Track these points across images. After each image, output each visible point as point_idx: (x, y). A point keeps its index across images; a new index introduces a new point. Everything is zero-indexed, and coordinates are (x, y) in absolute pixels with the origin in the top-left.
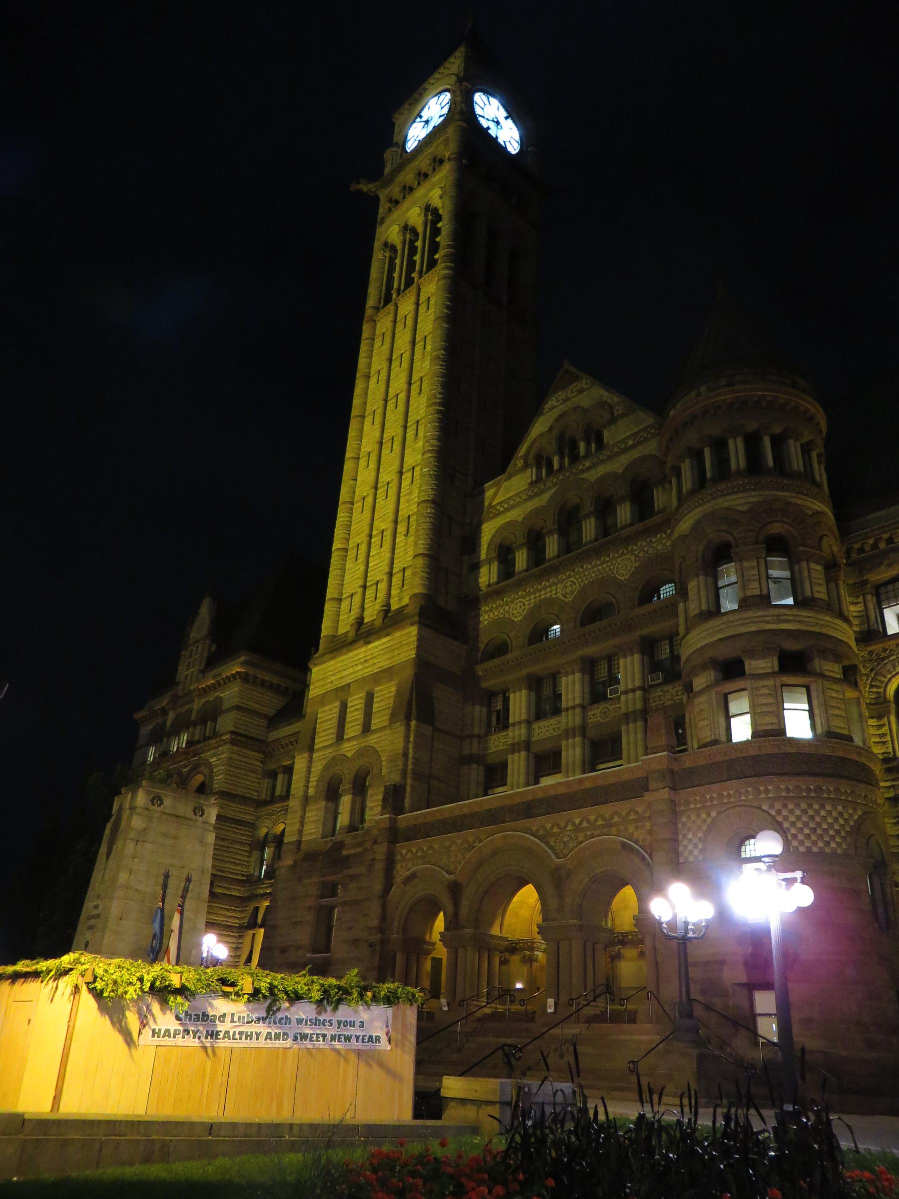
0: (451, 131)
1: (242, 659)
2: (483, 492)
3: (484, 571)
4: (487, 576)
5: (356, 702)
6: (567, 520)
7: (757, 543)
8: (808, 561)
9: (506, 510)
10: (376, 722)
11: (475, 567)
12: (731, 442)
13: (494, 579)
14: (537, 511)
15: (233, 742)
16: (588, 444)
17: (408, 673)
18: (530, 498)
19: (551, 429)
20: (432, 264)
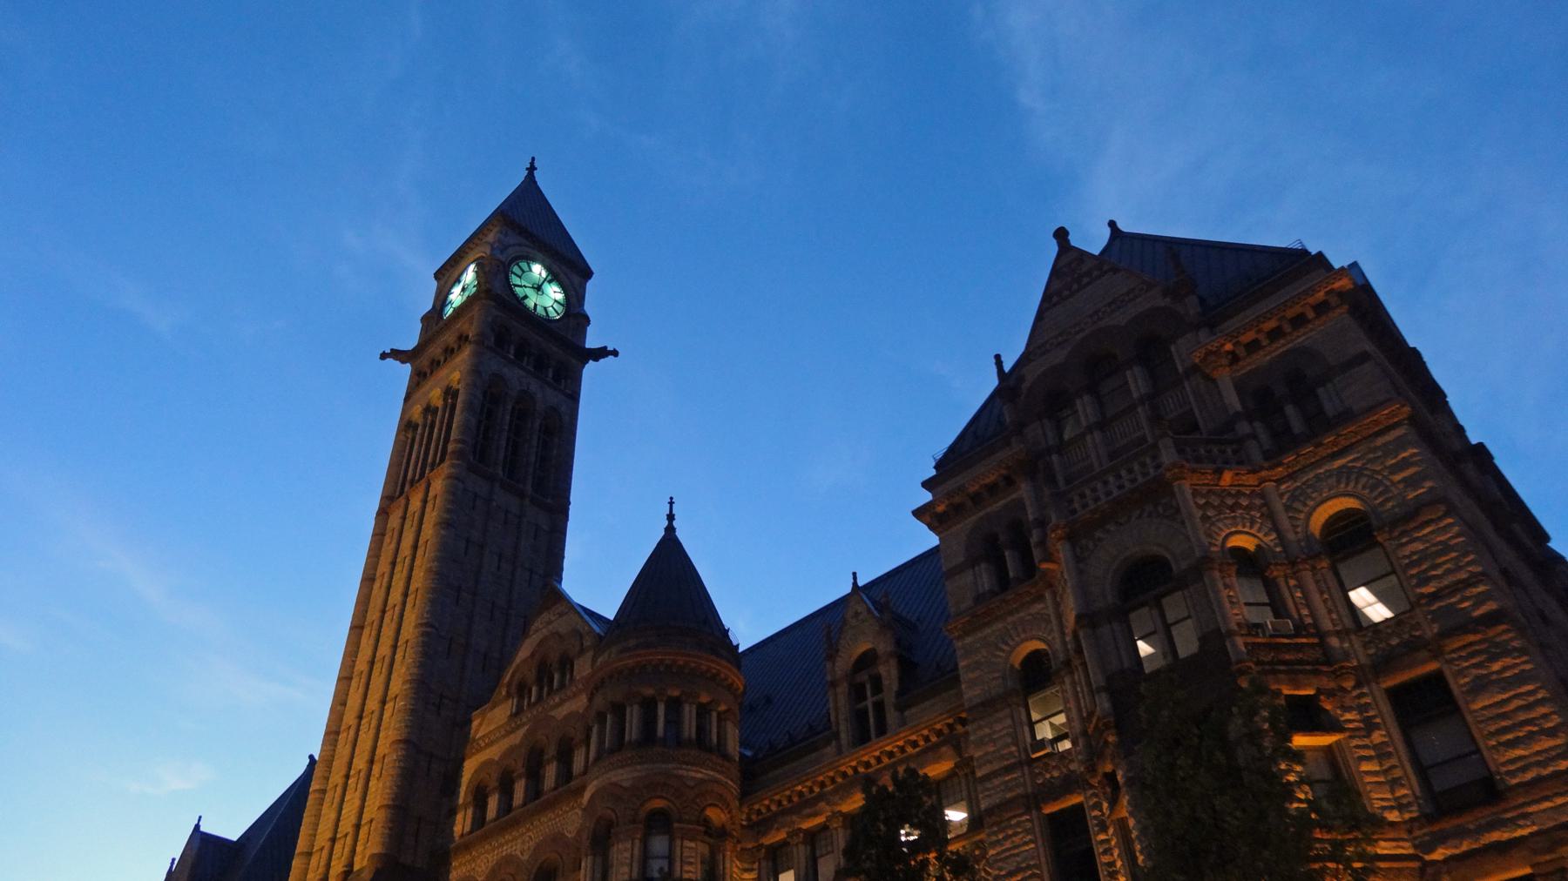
0: (476, 310)
2: (470, 721)
3: (459, 817)
4: (462, 824)
7: (634, 821)
8: (682, 839)
9: (488, 745)
11: (453, 812)
12: (628, 710)
13: (467, 829)
14: (511, 750)
16: (541, 689)
18: (508, 733)
19: (533, 655)
20: (442, 460)
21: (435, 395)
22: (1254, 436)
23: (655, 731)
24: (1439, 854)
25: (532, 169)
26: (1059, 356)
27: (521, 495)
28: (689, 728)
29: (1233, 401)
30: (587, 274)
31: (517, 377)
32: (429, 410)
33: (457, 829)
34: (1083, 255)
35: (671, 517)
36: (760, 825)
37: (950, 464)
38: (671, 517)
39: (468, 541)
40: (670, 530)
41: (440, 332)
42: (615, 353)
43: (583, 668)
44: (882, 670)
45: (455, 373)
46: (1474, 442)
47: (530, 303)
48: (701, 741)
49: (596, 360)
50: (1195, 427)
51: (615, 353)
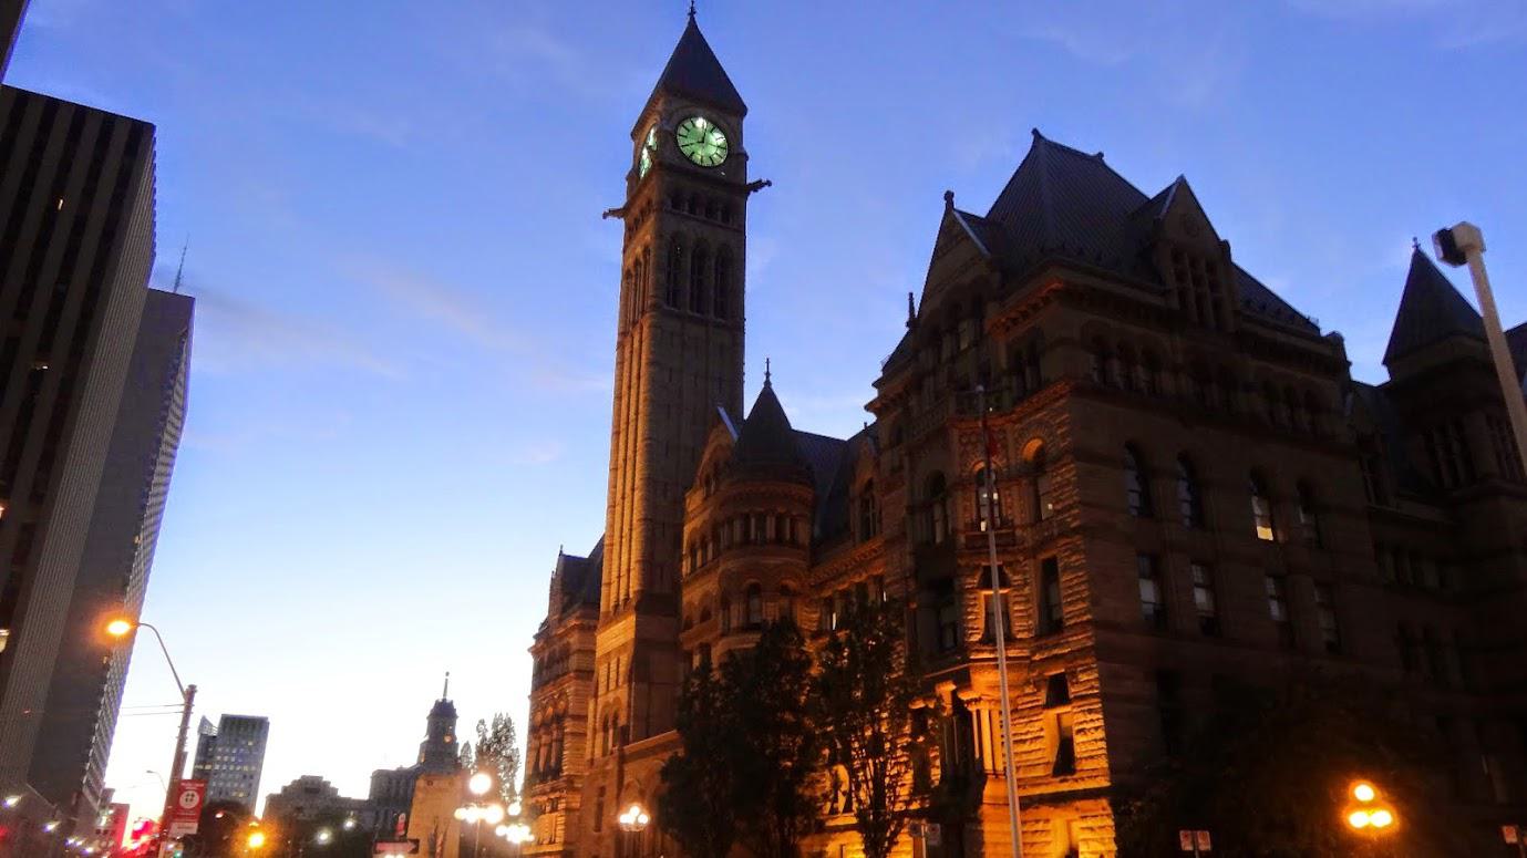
1: (578, 614)
2: (684, 500)
3: (684, 563)
4: (686, 567)
10: (620, 684)
15: (577, 678)
18: (705, 509)
19: (710, 459)
22: (1009, 388)
23: (749, 536)
24: (1037, 657)
25: (692, 13)
28: (771, 533)
31: (692, 229)
32: (637, 263)
33: (684, 570)
35: (768, 374)
36: (821, 586)
38: (768, 374)
39: (671, 370)
40: (768, 383)
41: (640, 191)
42: (769, 183)
45: (646, 235)
47: (697, 158)
48: (779, 539)
49: (756, 191)
51: (769, 183)
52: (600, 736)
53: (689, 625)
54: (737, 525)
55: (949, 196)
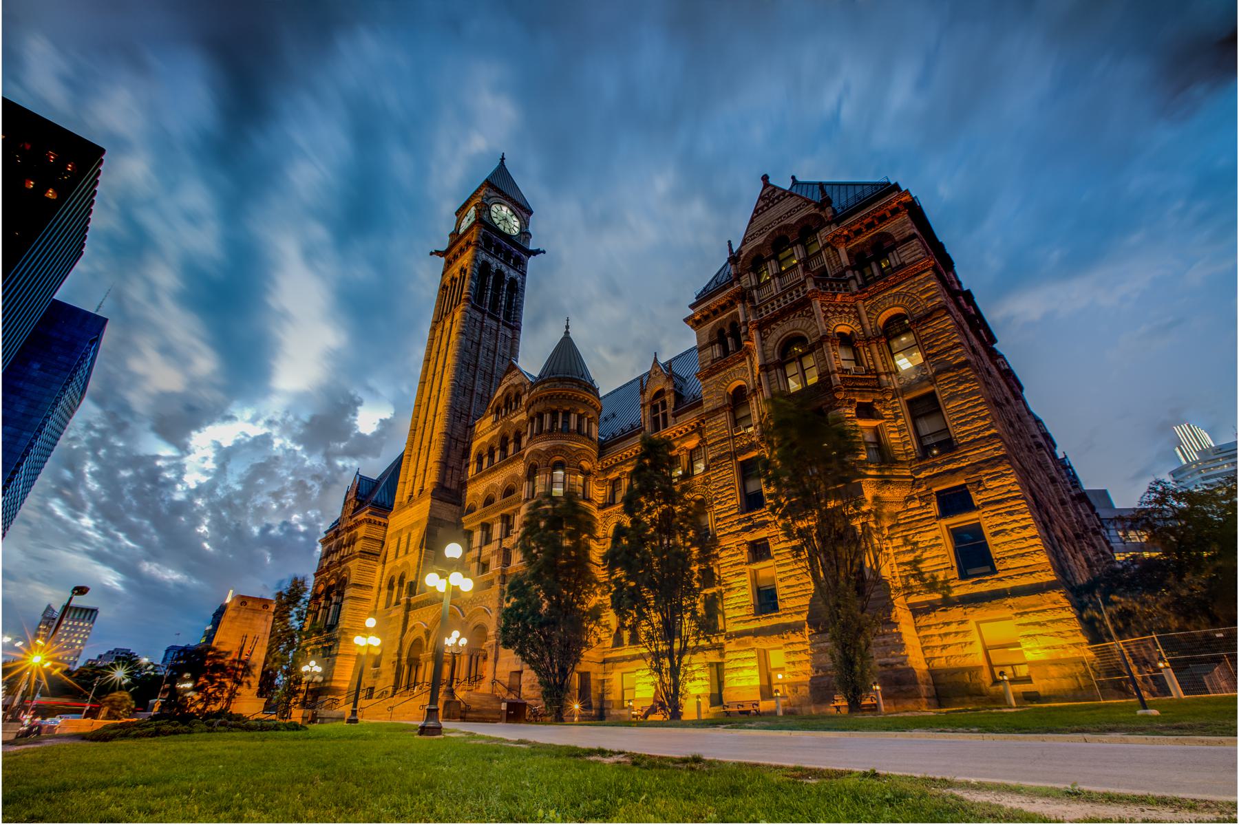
4: (472, 470)
5: (404, 538)
6: (504, 441)
11: (467, 465)
14: (494, 437)
17: (424, 524)
21: (455, 270)
22: (854, 278)
24: (923, 475)
25: (503, 159)
26: (760, 240)
27: (498, 320)
28: (573, 424)
29: (845, 259)
30: (530, 212)
31: (495, 264)
32: (453, 279)
33: (470, 473)
34: (775, 188)
35: (567, 327)
36: (606, 471)
37: (703, 297)
38: (567, 327)
40: (567, 333)
41: (458, 241)
43: (525, 398)
44: (667, 398)
45: (465, 260)
46: (965, 289)
48: (579, 430)
50: (825, 273)
52: (385, 592)
53: (471, 510)
54: (547, 418)
55: (765, 178)
